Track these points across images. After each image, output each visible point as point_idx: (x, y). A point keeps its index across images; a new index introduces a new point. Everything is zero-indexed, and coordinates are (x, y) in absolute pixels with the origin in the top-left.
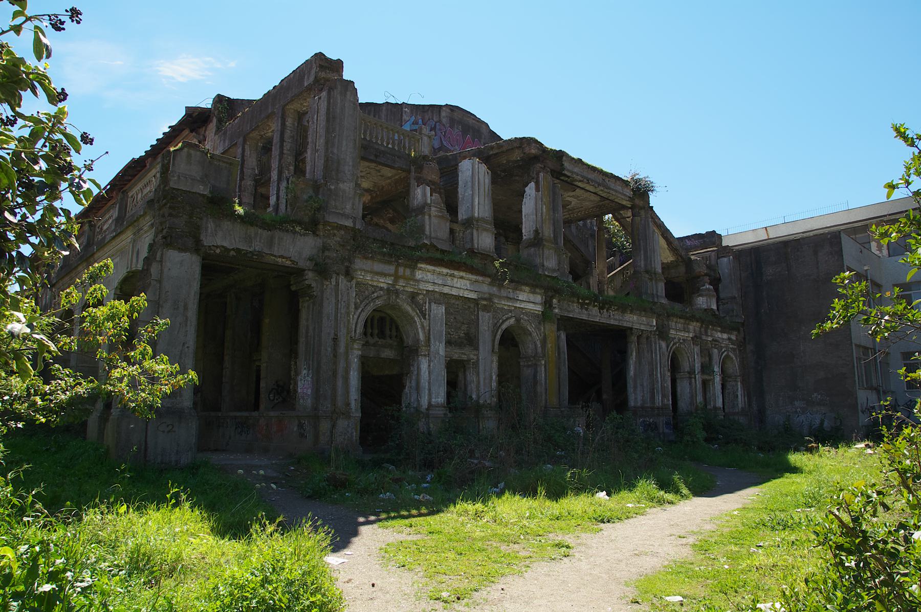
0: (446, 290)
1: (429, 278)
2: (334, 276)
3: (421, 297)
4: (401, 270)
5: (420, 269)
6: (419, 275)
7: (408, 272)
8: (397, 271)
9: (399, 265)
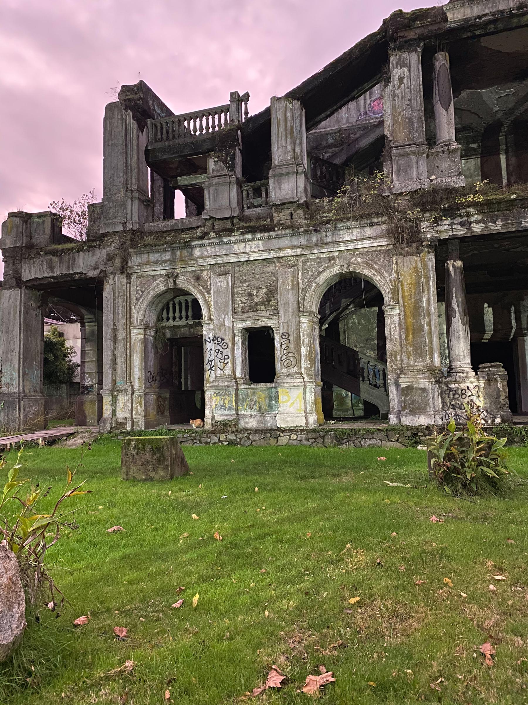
0: (232, 259)
2: (111, 277)
3: (205, 273)
6: (197, 252)
7: (185, 253)
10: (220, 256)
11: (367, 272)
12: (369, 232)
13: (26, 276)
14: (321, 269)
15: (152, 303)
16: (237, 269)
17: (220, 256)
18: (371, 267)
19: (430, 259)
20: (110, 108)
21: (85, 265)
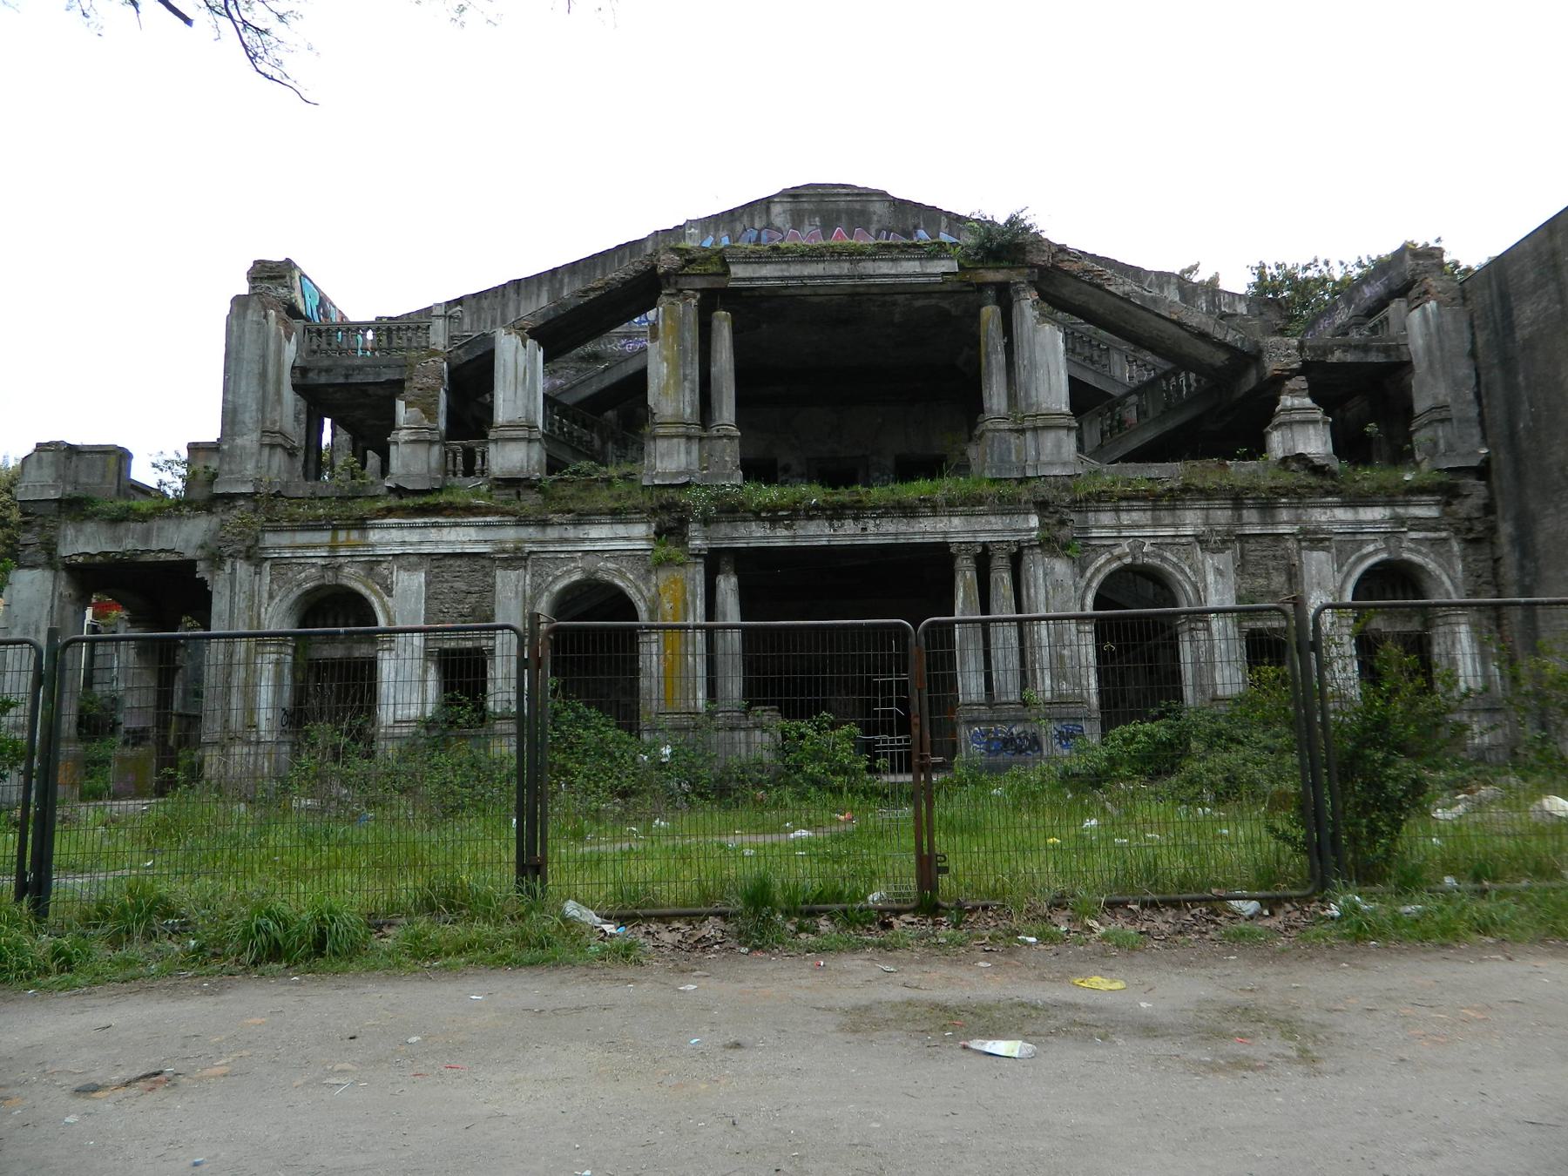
0: (426, 549)
1: (388, 537)
2: (229, 562)
3: (384, 565)
4: (342, 535)
5: (373, 527)
6: (374, 536)
8: (334, 538)
9: (335, 529)
10: (411, 544)
11: (617, 582)
12: (621, 530)
13: (65, 551)
14: (558, 573)
15: (296, 602)
16: (436, 563)
17: (411, 544)
18: (623, 576)
19: (698, 574)
20: (239, 302)
21: (183, 538)
